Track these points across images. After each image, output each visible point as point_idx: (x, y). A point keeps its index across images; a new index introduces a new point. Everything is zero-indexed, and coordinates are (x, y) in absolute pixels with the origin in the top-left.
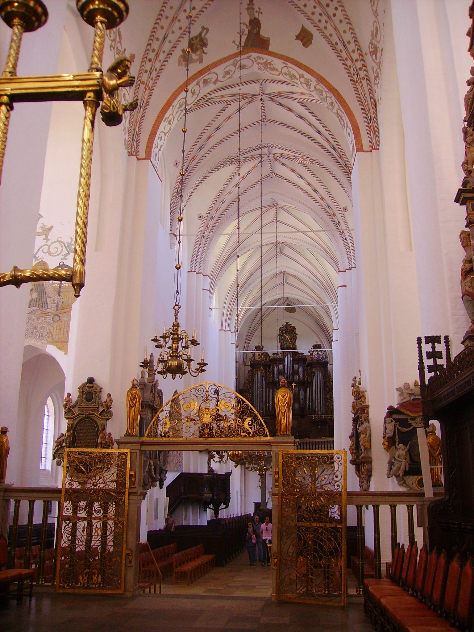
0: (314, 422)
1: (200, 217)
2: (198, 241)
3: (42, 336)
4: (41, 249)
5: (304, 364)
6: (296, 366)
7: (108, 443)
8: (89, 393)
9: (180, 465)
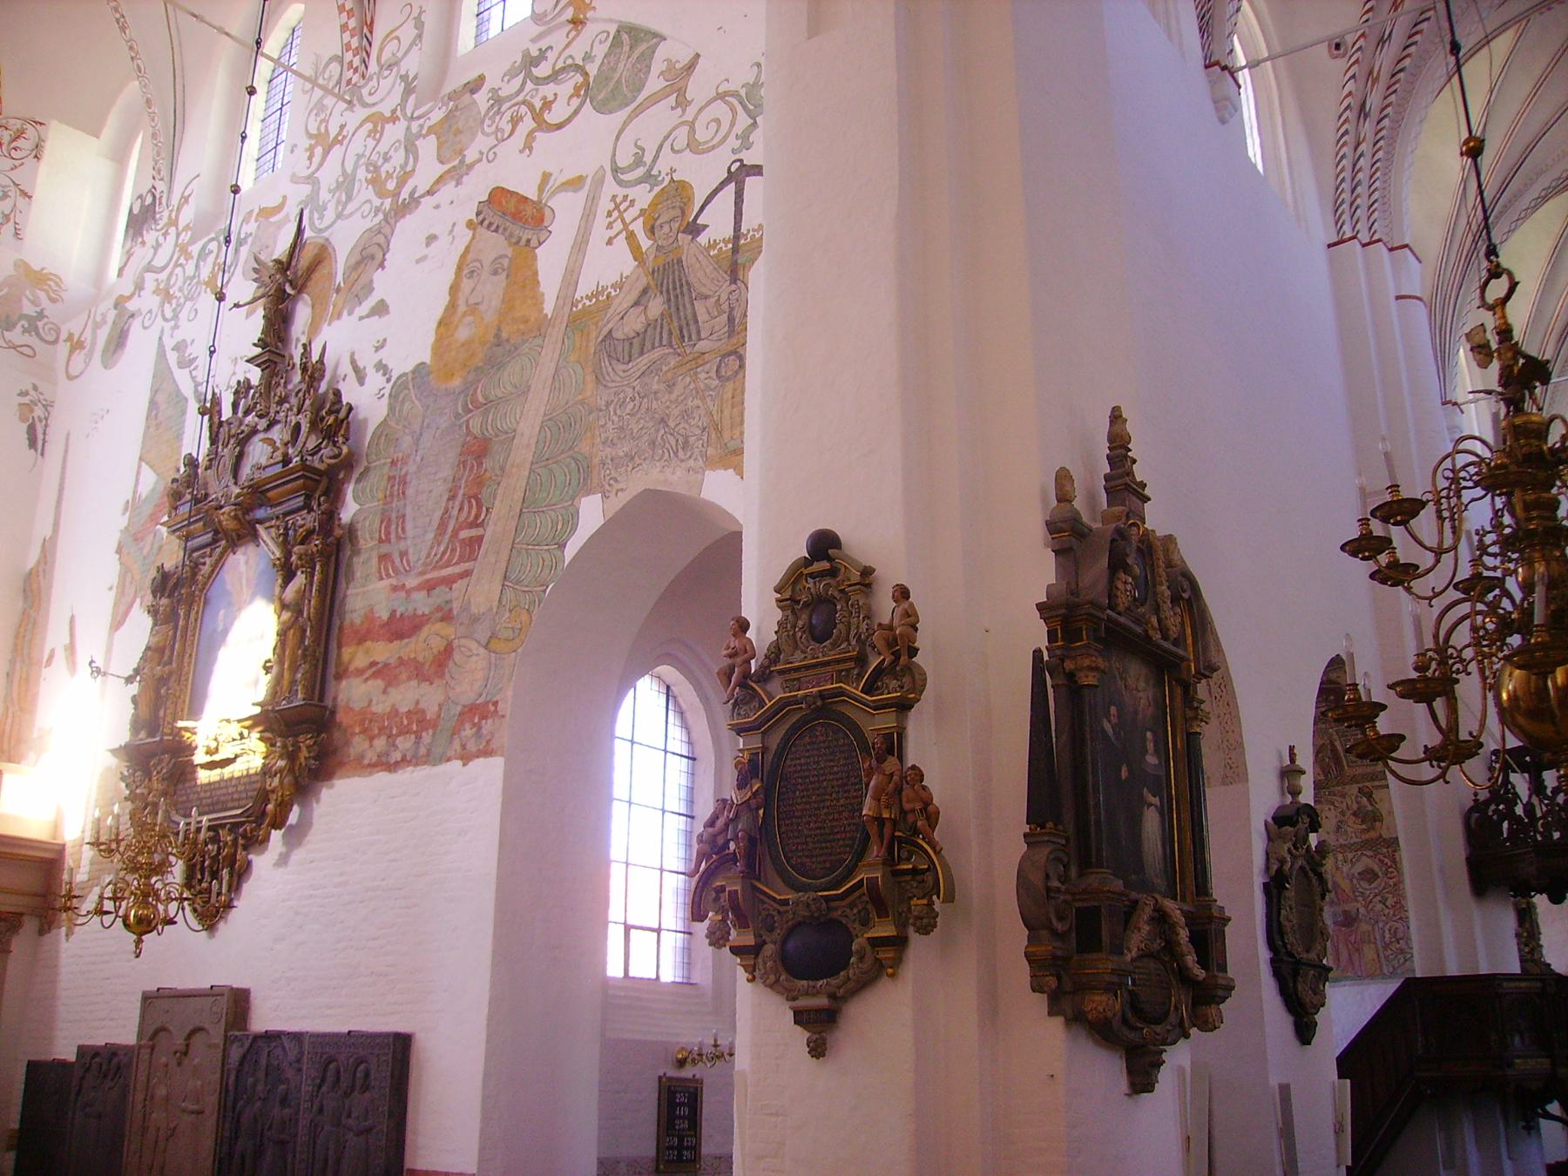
1: (1338, 46)
2: (1346, 132)
3: (686, 445)
4: (667, 145)
7: (910, 818)
8: (821, 602)
9: (1402, 951)
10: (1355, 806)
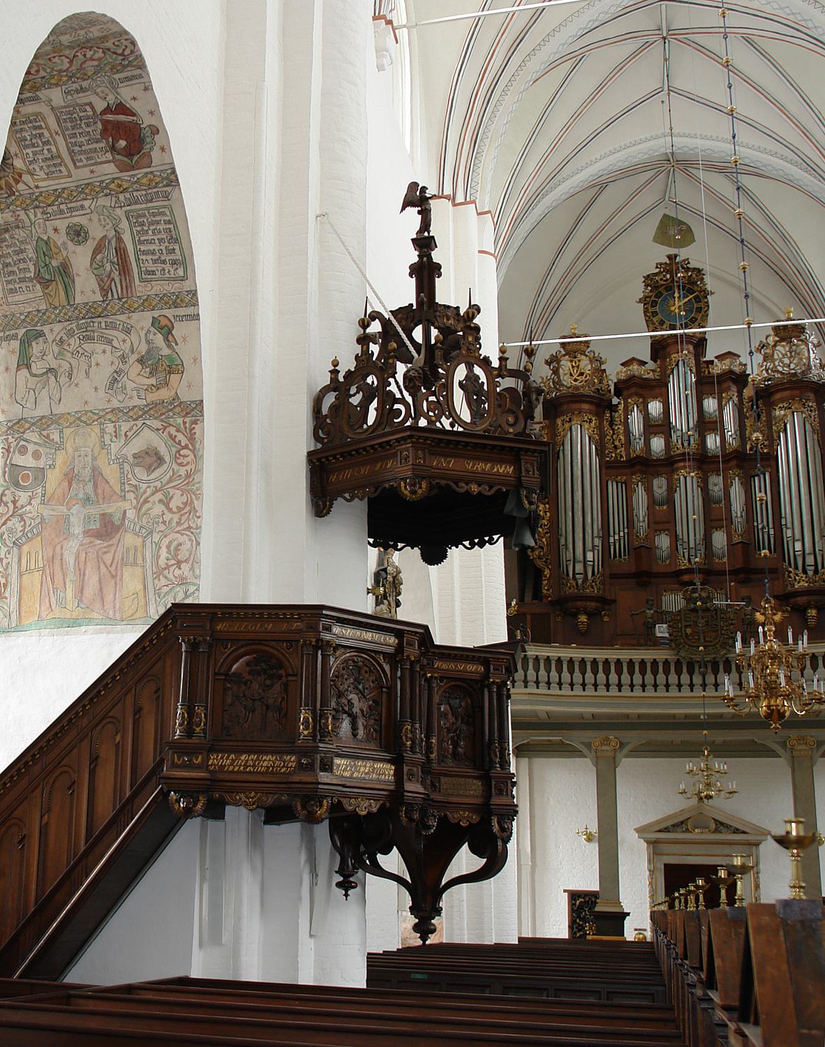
6: (710, 404)
9: (183, 581)
10: (143, 348)
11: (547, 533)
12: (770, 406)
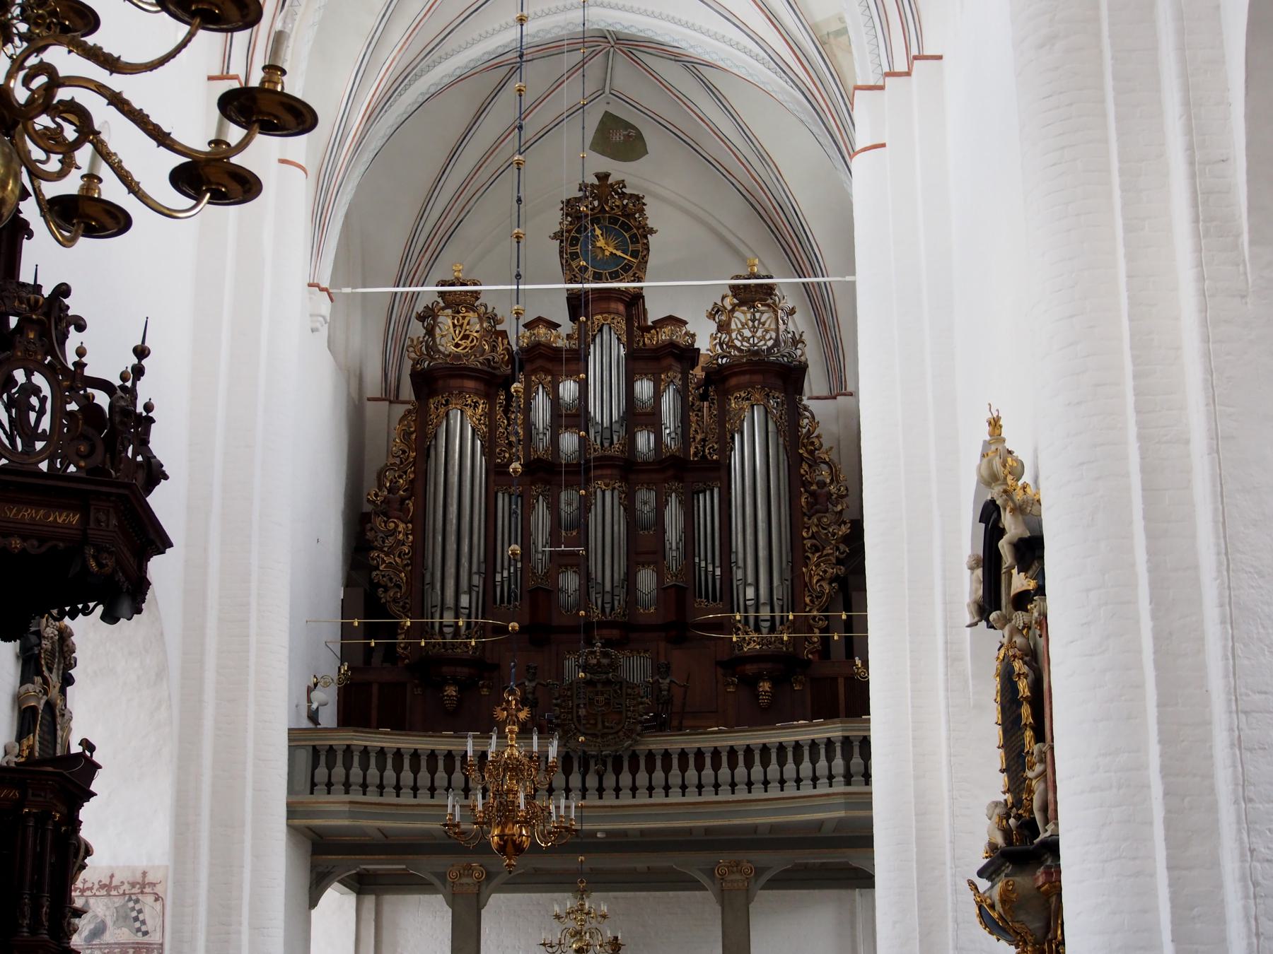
0: (734, 664)
5: (685, 379)
6: (644, 388)
11: (407, 565)
12: (725, 394)
